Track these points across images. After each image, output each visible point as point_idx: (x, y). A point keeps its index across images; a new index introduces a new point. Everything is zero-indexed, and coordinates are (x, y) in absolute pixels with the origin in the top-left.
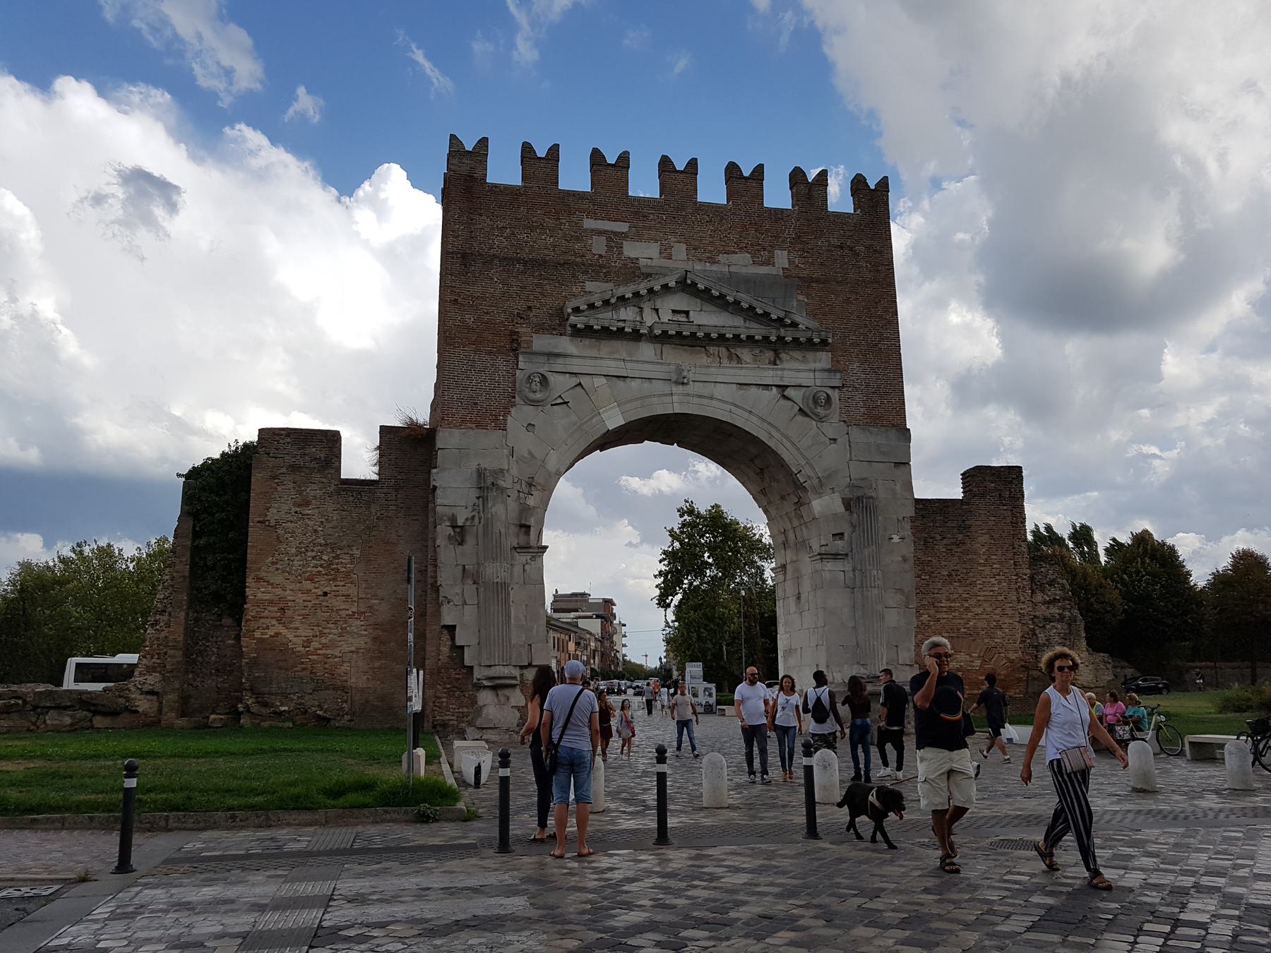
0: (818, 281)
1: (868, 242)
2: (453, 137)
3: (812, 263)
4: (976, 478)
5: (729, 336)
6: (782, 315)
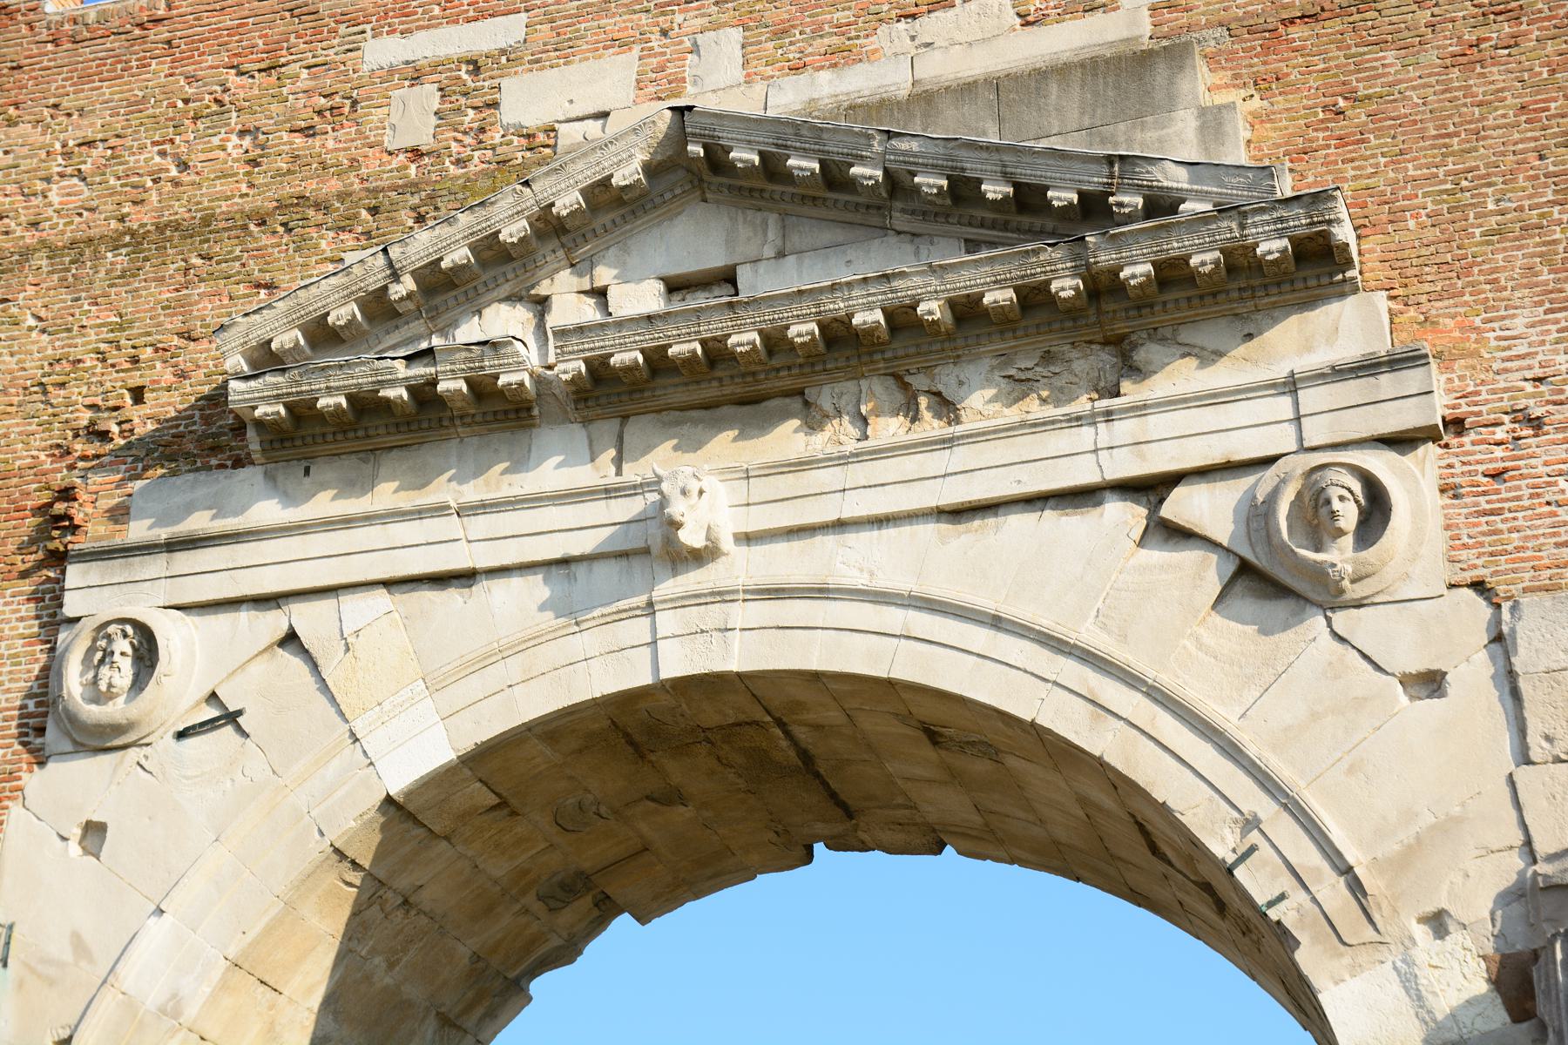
5: (869, 317)
6: (1095, 180)
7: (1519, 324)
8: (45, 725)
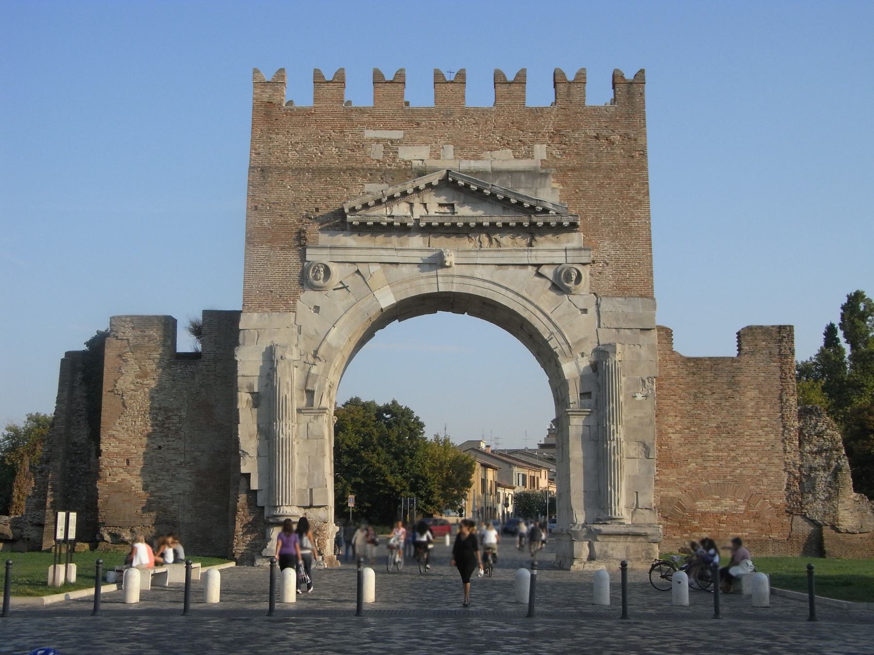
0: (573, 170)
1: (623, 131)
2: (256, 71)
3: (569, 154)
6: (533, 203)
7: (606, 244)
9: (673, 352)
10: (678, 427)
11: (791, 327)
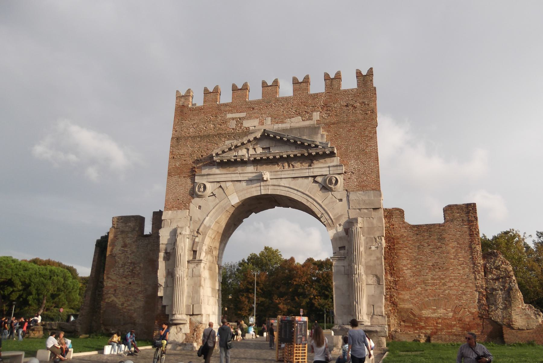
0: (333, 124)
2: (177, 91)
4: (449, 210)
6: (309, 143)
8: (193, 194)
9: (404, 222)
10: (409, 266)
11: (475, 204)
